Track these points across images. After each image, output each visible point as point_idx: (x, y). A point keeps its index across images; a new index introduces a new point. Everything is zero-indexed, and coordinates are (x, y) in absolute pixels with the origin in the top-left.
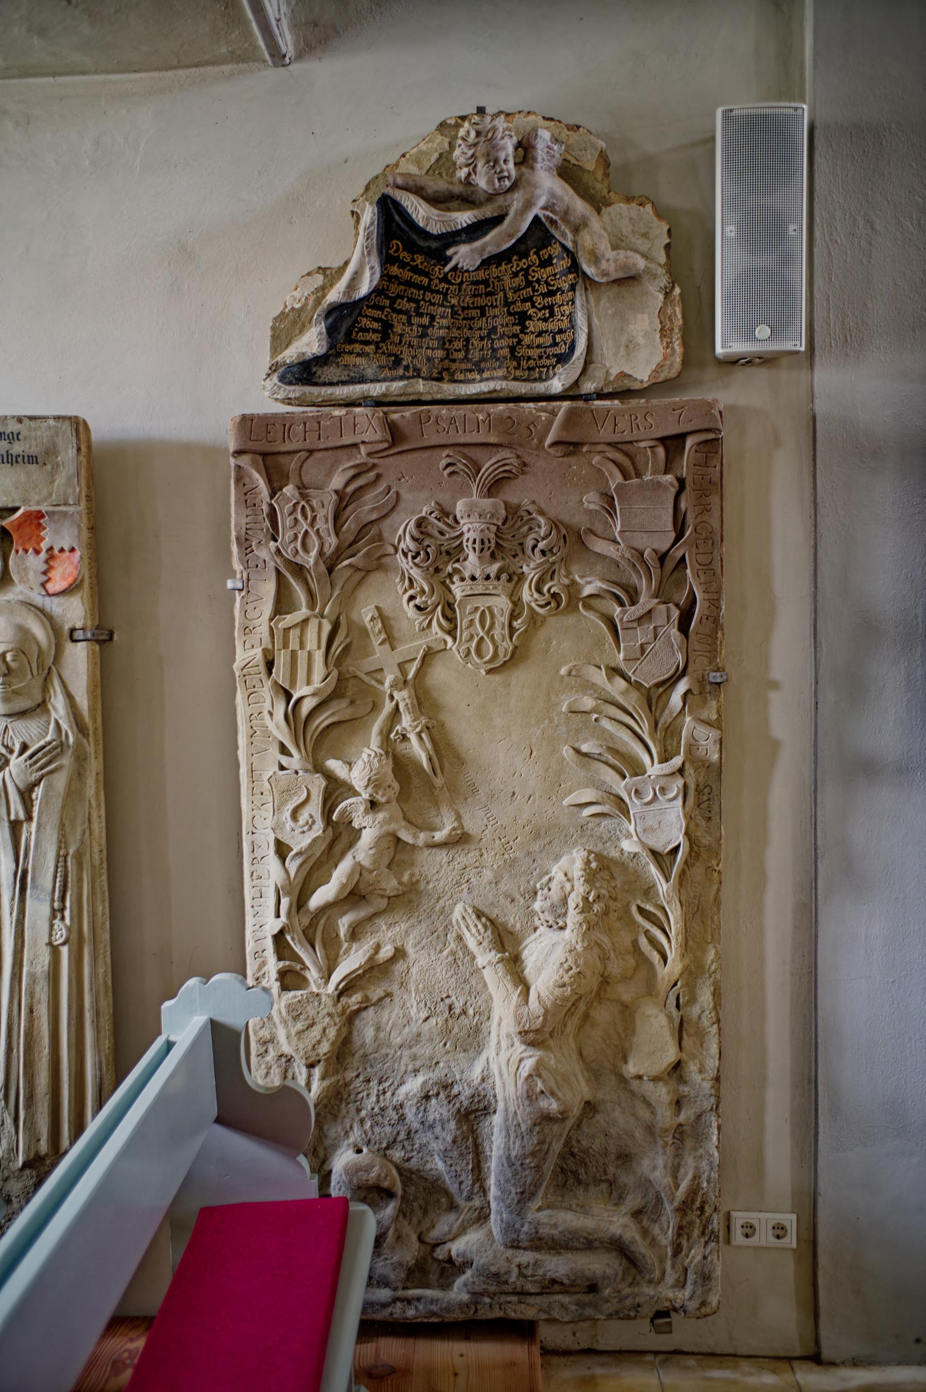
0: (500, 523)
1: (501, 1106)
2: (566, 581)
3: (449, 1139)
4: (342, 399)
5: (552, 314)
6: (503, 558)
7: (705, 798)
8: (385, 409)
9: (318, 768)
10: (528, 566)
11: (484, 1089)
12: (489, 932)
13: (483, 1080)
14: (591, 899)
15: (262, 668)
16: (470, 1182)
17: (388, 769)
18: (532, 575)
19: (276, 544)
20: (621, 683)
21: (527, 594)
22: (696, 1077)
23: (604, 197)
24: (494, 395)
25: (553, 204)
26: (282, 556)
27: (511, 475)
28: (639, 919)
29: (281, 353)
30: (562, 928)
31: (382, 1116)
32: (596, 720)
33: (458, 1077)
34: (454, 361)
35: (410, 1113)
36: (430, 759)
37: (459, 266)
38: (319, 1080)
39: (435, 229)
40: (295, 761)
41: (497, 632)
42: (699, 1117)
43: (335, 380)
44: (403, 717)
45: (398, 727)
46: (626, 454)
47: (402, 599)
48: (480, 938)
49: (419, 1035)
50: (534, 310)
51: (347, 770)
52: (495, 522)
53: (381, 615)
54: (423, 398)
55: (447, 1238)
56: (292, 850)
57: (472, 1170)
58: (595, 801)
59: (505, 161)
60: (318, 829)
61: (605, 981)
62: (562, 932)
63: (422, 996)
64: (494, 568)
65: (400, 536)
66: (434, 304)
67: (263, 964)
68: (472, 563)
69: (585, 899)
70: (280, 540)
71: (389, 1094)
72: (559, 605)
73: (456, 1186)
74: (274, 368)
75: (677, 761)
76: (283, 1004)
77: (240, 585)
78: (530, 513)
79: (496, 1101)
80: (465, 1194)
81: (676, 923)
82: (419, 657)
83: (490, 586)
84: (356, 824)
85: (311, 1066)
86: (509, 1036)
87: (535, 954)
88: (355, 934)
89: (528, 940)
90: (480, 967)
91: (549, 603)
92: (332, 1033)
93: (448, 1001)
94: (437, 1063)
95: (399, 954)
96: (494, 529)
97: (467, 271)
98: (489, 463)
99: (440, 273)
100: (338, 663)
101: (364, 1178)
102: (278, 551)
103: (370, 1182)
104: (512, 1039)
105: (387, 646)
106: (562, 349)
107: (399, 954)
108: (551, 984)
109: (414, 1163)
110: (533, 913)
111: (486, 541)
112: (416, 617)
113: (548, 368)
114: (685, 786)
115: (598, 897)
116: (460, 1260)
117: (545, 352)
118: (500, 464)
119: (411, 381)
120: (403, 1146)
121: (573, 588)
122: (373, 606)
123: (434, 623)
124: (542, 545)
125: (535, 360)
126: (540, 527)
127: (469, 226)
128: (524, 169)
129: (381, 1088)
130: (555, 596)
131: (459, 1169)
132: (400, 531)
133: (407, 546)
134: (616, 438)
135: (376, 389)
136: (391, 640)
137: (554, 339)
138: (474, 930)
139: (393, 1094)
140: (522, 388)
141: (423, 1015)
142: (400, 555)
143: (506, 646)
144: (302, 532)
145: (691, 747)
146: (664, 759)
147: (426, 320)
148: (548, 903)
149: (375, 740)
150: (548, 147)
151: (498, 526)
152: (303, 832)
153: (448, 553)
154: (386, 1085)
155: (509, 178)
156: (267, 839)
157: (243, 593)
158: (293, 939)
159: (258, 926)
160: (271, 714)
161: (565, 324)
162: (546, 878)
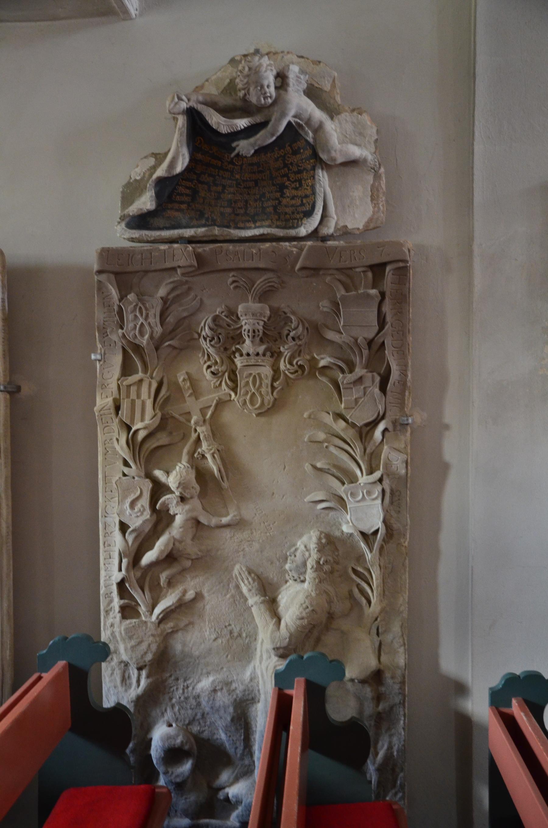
0: (266, 320)
1: (262, 697)
2: (308, 357)
3: (229, 719)
4: (166, 239)
5: (301, 185)
6: (268, 342)
7: (396, 499)
8: (194, 245)
9: (149, 476)
10: (284, 347)
11: (252, 686)
12: (256, 583)
13: (251, 680)
14: (321, 563)
15: (113, 411)
16: (242, 748)
17: (192, 476)
18: (286, 353)
19: (122, 331)
20: (342, 423)
21: (283, 366)
22: (389, 681)
23: (336, 109)
24: (264, 237)
25: (300, 114)
26: (126, 338)
27: (274, 289)
28: (354, 576)
29: (127, 208)
30: (303, 581)
31: (186, 703)
32: (327, 447)
33: (235, 678)
34: (237, 215)
35: (204, 701)
36: (220, 471)
37: (240, 154)
38: (145, 678)
40: (133, 470)
41: (263, 390)
42: (392, 708)
43: (161, 226)
44: (203, 443)
45: (199, 450)
46: (348, 276)
47: (203, 368)
48: (250, 587)
49: (210, 650)
50: (289, 182)
51: (165, 477)
52: (263, 319)
53: (190, 377)
54: (218, 239)
55: (227, 784)
56: (129, 527)
57: (243, 740)
58: (324, 499)
59: (268, 86)
60: (147, 514)
61: (331, 616)
62: (303, 584)
63: (213, 624)
64: (261, 349)
65: (202, 327)
66: (223, 178)
67: (111, 601)
68: (248, 346)
69: (318, 562)
70: (125, 329)
71: (190, 688)
72: (303, 372)
73: (233, 750)
74: (122, 218)
75: (377, 475)
76: (123, 628)
77: (99, 357)
78: (285, 313)
79: (260, 694)
80: (239, 755)
81: (377, 579)
82: (213, 405)
83: (260, 360)
84: (171, 512)
85: (140, 669)
86: (267, 651)
87: (286, 598)
88: (170, 583)
89: (282, 589)
90: (250, 605)
91: (297, 371)
92: (154, 647)
93: (229, 628)
94: (222, 668)
95: (199, 596)
96: (262, 323)
97: (246, 157)
98: (260, 281)
99: (228, 158)
100: (162, 408)
101: (173, 743)
102: (124, 336)
103: (176, 746)
104: (270, 653)
105: (193, 398)
106: (308, 208)
107: (199, 596)
108: (295, 617)
109: (206, 735)
110: (286, 571)
111: (256, 331)
112: (211, 379)
113: (298, 220)
114: (383, 491)
115: (326, 562)
116: (234, 800)
117: (296, 210)
118: (266, 282)
119: (210, 228)
120: (199, 723)
121: (313, 362)
122: (184, 372)
123: (223, 383)
124: (292, 334)
125: (289, 214)
126: (292, 322)
127: (245, 128)
128: (282, 92)
129: (185, 684)
130: (301, 367)
131: (235, 739)
132: (202, 324)
133: (206, 334)
134: (340, 265)
135: (188, 233)
136: (196, 393)
137: (302, 201)
138: (246, 582)
139: (193, 688)
140: (280, 233)
141: (213, 637)
142: (202, 340)
143: (269, 399)
144: (139, 323)
145: (387, 465)
146: (371, 472)
147: (220, 189)
148: (295, 564)
149: (185, 458)
150: (297, 77)
151: (264, 321)
152: (138, 517)
153: (233, 338)
154: (189, 682)
155: (271, 97)
156: (114, 521)
157: (101, 363)
158: (130, 586)
159: (108, 577)
160: (118, 440)
161: (309, 192)
162: (293, 549)
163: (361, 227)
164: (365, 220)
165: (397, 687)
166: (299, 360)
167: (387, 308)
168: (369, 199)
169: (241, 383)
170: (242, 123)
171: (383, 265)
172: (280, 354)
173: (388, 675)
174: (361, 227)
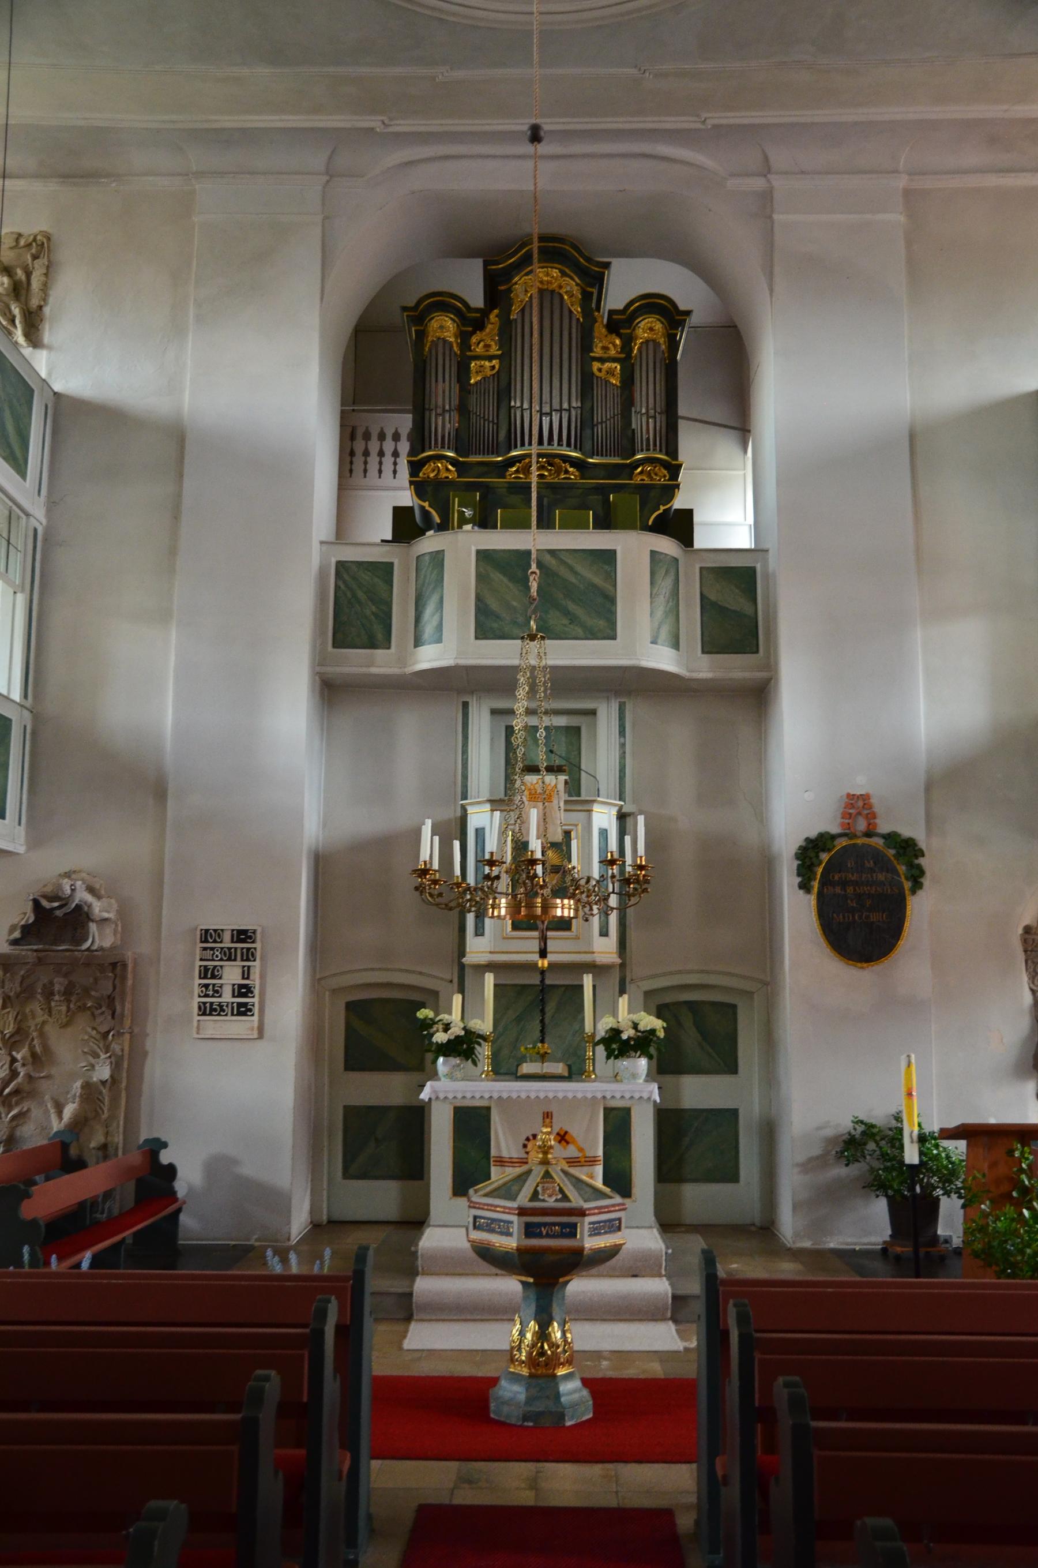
17: (28, 1055)
21: (72, 1006)
28: (97, 1101)
39: (48, 907)
60: (7, 1072)
68: (57, 998)
75: (108, 1054)
88: (17, 1104)
92: (7, 1133)
95: (29, 1110)
114: (111, 1063)
115: (85, 1094)
121: (85, 1005)
130: (79, 1007)
135: (35, 947)
136: (34, 1017)
143: (65, 1020)
146: (106, 1053)
164: (111, 943)
166: (78, 1004)
167: (117, 982)
169: (53, 1013)
170: (56, 904)
171: (116, 963)
172: (71, 1001)
173: (109, 1145)
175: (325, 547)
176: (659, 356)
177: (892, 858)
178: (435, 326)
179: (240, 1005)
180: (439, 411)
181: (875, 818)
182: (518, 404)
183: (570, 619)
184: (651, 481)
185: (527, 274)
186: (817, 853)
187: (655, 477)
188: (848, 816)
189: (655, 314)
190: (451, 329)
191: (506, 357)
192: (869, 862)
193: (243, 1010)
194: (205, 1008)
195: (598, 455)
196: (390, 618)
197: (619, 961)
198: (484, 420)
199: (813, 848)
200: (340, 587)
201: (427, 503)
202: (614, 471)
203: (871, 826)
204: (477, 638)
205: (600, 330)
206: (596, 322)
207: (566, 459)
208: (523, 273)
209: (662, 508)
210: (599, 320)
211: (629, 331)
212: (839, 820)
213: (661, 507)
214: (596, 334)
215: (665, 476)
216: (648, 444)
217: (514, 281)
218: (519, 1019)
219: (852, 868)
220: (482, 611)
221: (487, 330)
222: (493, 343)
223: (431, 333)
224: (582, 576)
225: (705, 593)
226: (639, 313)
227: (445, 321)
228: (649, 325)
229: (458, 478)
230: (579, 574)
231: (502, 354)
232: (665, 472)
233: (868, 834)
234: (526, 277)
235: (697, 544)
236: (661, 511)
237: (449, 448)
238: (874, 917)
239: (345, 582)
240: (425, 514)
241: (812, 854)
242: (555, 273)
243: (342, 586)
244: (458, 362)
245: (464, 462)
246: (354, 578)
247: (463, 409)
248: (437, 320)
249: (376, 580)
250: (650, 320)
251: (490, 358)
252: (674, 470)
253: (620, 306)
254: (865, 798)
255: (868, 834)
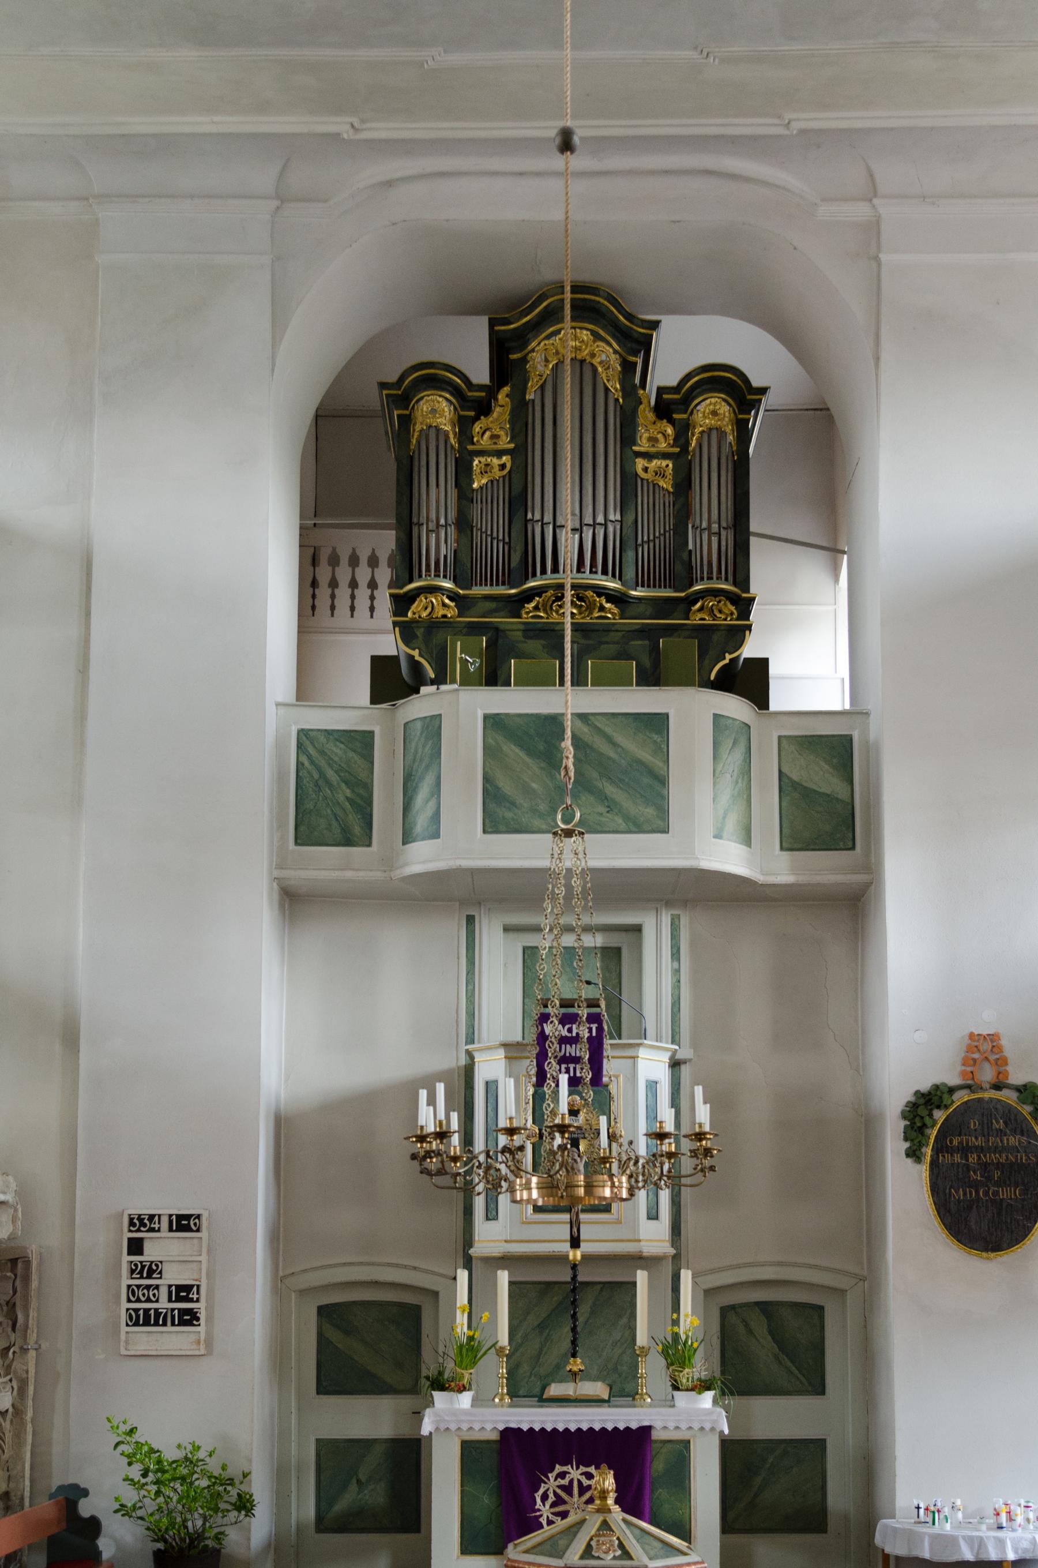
22: (14, 1498)
75: (9, 1377)
145: (15, 1372)
163: (6, 1238)
164: (8, 1234)
165: (17, 1501)
167: (18, 1283)
168: (11, 1222)
171: (17, 1259)
173: (12, 1494)
174: (6, 1238)
175: (282, 711)
176: (726, 450)
177: (1029, 1117)
178: (425, 409)
179: (183, 1312)
180: (432, 526)
181: (1006, 1064)
182: (537, 516)
183: (608, 807)
184: (714, 620)
185: (548, 337)
186: (931, 1110)
187: (719, 615)
188: (972, 1062)
189: (720, 391)
190: (447, 414)
191: (520, 452)
192: (998, 1122)
193: (189, 1318)
194: (138, 1316)
195: (643, 586)
196: (370, 804)
197: (673, 1251)
198: (492, 539)
199: (926, 1104)
200: (303, 764)
201: (417, 651)
202: (664, 607)
203: (1001, 1076)
204: (485, 832)
205: (645, 414)
206: (641, 403)
207: (600, 591)
208: (544, 335)
209: (728, 657)
210: (645, 401)
211: (685, 416)
212: (960, 1068)
213: (727, 655)
214: (641, 420)
215: (732, 614)
216: (710, 572)
217: (530, 348)
218: (542, 1327)
219: (975, 1130)
220: (492, 794)
221: (495, 415)
222: (502, 433)
223: (420, 419)
224: (623, 749)
225: (785, 770)
226: (698, 390)
227: (438, 402)
228: (712, 407)
229: (459, 616)
230: (621, 747)
231: (515, 447)
232: (733, 608)
233: (997, 1087)
234: (547, 342)
235: (775, 705)
236: (727, 661)
237: (445, 577)
238: (1004, 1194)
239: (310, 757)
240: (415, 667)
241: (922, 1111)
242: (585, 335)
243: (307, 763)
244: (456, 459)
245: (465, 597)
246: (322, 753)
247: (463, 524)
248: (427, 401)
249: (351, 754)
250: (713, 400)
251: (499, 454)
252: (744, 605)
253: (673, 382)
254: (993, 1039)
255: (997, 1087)
